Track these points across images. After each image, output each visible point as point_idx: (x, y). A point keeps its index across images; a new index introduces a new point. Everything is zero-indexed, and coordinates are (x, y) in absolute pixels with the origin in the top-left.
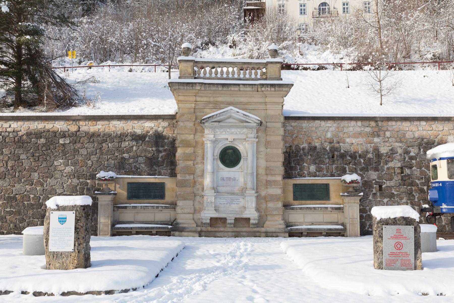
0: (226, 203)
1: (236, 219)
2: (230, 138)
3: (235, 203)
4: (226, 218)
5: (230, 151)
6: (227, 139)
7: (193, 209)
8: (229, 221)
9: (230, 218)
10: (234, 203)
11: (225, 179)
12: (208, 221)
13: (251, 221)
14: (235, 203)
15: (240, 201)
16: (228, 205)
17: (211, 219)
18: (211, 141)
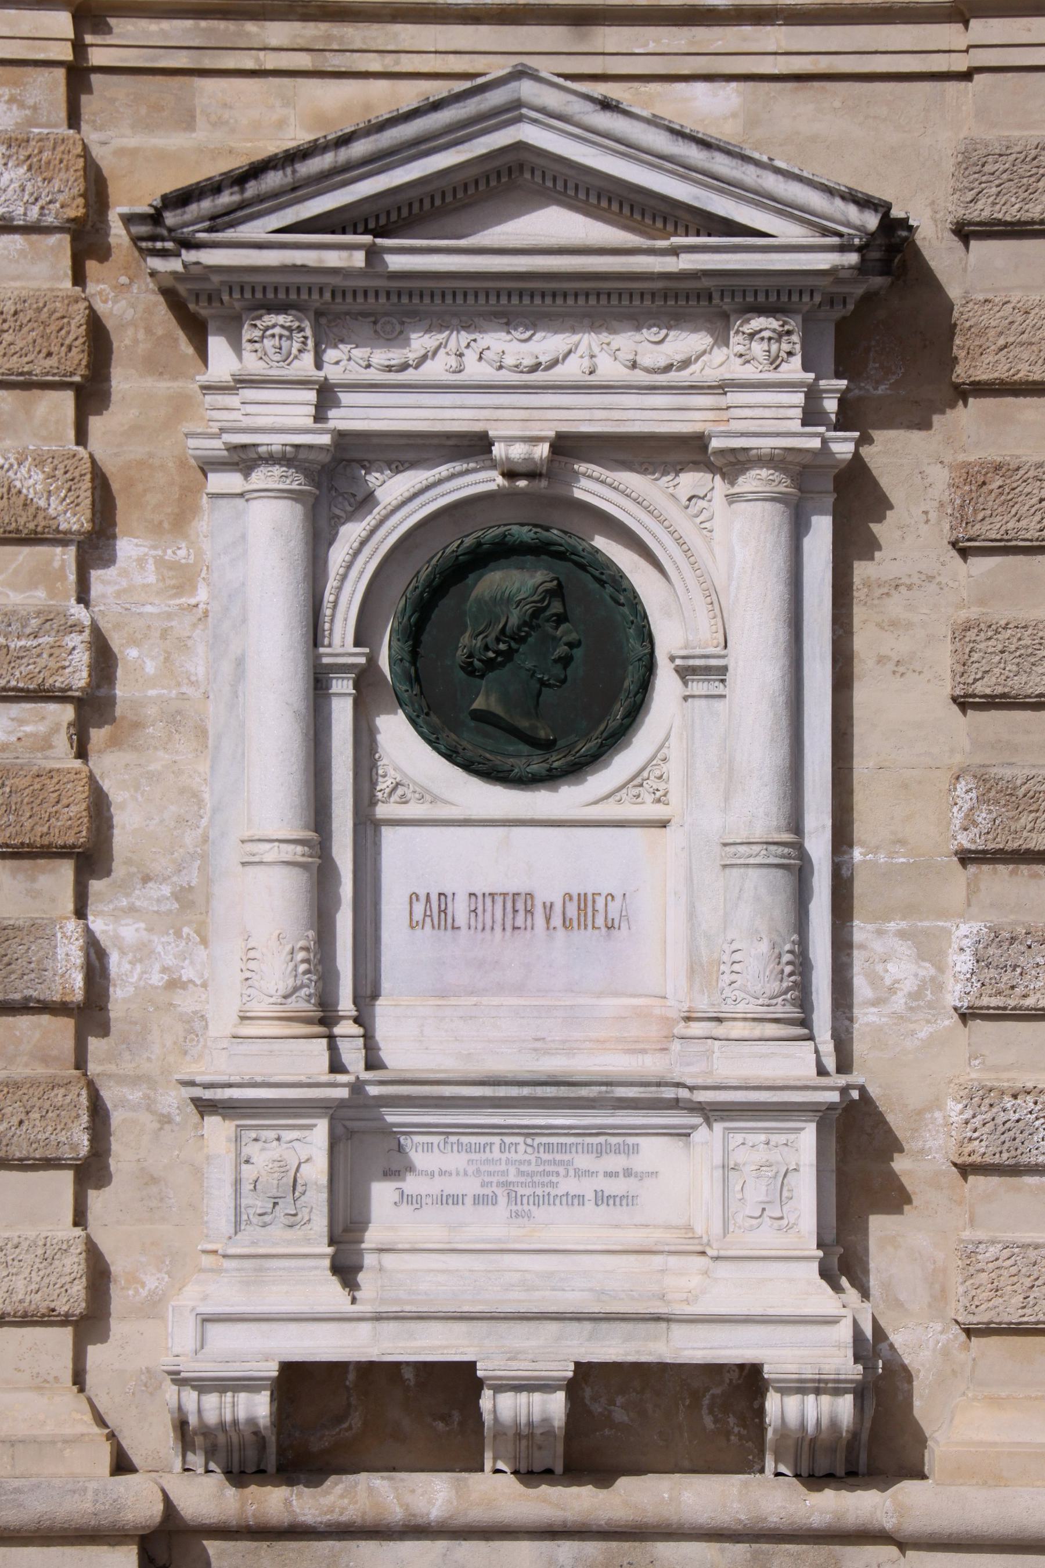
0: (471, 1186)
1: (586, 1381)
2: (521, 431)
3: (587, 1187)
4: (472, 1365)
5: (515, 583)
6: (474, 446)
7: (74, 1263)
8: (499, 1407)
9: (521, 1369)
10: (569, 1185)
11: (460, 910)
12: (259, 1407)
13: (772, 1403)
14: (587, 1187)
15: (638, 1163)
16: (502, 1210)
17: (295, 1381)
18: (289, 458)
